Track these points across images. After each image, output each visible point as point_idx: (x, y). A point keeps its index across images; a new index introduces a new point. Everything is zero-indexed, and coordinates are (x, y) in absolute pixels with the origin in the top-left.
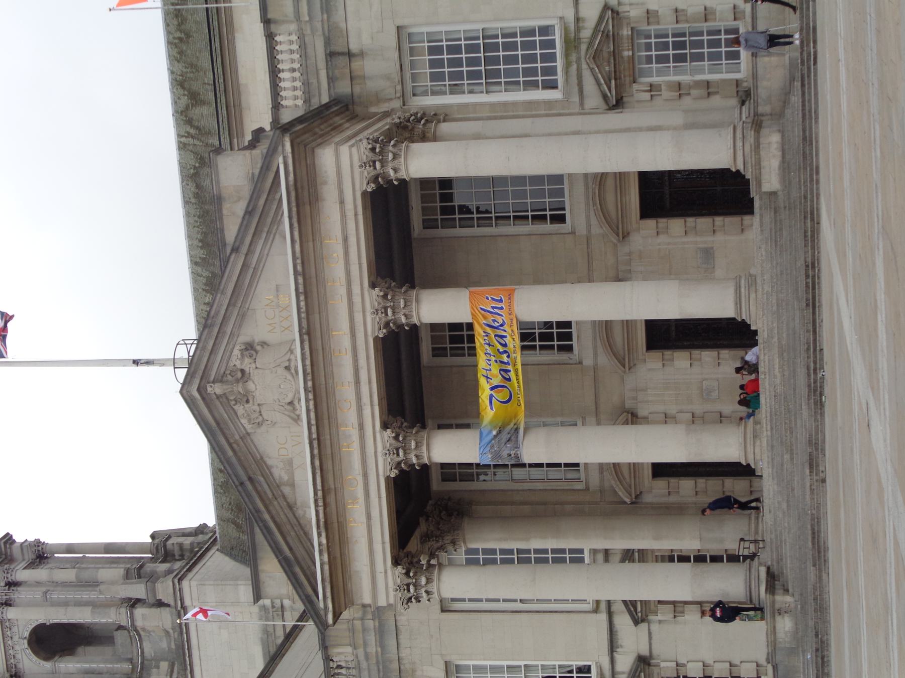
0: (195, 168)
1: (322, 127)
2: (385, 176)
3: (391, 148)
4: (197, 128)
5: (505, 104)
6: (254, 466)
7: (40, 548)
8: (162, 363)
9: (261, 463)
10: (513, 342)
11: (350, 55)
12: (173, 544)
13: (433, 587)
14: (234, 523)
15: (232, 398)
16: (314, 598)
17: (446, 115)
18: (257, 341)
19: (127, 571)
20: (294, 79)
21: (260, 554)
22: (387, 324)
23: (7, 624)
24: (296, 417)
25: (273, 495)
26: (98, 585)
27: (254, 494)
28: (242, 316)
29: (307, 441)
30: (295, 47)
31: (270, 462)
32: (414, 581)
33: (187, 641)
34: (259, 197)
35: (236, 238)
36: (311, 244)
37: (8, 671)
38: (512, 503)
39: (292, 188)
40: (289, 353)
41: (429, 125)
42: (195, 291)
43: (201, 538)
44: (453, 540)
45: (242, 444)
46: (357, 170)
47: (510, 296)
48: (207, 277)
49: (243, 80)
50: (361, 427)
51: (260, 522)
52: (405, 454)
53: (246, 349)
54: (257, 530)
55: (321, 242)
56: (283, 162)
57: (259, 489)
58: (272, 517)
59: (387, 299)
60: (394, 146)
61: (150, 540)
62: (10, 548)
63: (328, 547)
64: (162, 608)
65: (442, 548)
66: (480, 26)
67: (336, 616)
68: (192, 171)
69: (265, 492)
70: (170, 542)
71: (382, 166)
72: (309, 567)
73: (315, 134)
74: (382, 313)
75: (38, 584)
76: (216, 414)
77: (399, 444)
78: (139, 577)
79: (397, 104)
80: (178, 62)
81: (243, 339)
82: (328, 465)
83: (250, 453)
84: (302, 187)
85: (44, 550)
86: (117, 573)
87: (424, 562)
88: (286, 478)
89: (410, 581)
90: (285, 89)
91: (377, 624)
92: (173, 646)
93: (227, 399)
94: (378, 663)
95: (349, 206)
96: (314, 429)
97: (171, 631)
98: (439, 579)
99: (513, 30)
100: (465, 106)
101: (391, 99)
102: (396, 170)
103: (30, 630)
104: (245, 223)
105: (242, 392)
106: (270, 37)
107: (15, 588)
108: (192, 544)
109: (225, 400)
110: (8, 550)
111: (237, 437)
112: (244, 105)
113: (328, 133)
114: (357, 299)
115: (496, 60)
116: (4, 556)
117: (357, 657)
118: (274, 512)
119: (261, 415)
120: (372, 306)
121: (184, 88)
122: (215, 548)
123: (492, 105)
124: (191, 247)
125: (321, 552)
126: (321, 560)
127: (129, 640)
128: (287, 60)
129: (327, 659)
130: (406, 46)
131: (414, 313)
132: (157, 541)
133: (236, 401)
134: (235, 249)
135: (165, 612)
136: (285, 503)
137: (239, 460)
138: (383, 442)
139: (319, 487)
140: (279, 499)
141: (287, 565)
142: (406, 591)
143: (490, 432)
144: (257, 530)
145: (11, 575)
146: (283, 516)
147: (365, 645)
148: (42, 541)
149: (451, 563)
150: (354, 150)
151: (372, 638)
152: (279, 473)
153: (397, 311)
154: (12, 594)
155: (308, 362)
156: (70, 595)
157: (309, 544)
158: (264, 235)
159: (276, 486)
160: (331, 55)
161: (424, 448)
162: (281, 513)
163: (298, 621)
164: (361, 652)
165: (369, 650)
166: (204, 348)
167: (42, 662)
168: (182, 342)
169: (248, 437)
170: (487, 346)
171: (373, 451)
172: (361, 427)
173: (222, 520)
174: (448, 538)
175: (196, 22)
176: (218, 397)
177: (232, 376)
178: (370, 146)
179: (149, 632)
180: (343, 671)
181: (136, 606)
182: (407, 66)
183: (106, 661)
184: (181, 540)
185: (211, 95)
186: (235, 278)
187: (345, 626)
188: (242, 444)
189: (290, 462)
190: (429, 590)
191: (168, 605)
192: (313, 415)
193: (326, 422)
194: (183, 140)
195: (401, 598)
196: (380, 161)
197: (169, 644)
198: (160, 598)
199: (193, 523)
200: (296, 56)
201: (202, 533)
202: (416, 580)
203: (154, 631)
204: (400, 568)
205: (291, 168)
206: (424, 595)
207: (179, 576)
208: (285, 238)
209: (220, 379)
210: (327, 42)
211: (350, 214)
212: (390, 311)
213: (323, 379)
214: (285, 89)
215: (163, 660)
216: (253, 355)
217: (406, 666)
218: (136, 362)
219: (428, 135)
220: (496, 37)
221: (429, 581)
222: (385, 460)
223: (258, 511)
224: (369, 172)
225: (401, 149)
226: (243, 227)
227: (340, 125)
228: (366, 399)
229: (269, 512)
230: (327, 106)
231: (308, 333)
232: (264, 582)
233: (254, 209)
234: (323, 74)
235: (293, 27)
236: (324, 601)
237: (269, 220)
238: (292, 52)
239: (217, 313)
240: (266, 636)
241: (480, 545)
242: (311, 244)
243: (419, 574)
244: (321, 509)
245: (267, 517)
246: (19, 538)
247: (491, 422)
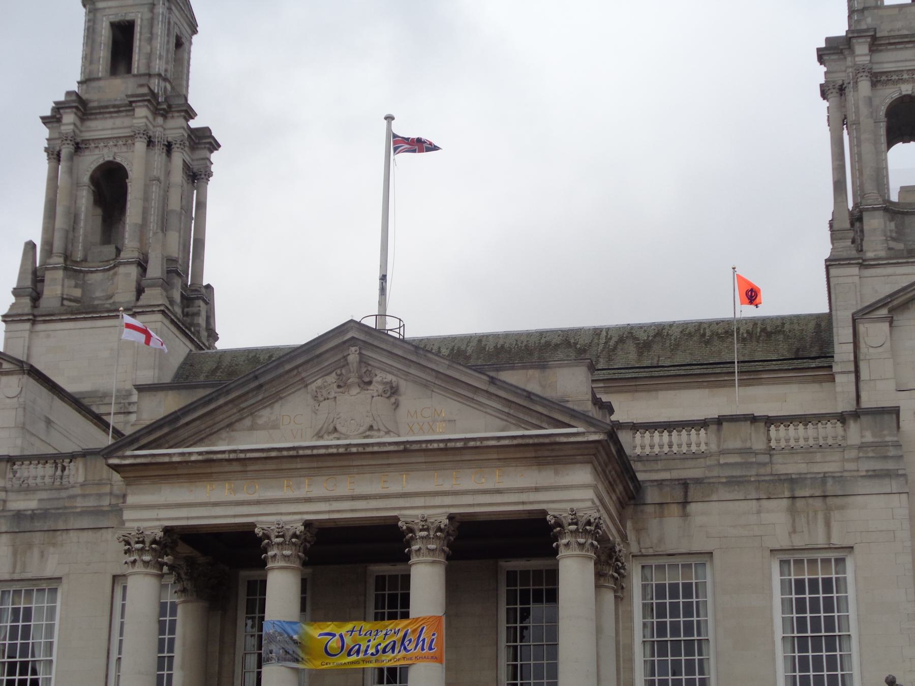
0: (576, 344)
1: (613, 473)
2: (561, 534)
3: (590, 541)
4: (615, 348)
5: (631, 660)
6: (274, 390)
7: (203, 176)
8: (382, 303)
9: (277, 397)
10: (388, 661)
11: (685, 503)
12: (200, 307)
13: (138, 568)
14: (217, 368)
15: (344, 371)
16: (136, 446)
17: (622, 599)
18: (400, 398)
19: (174, 260)
20: (661, 446)
21: (184, 393)
22: (411, 530)
23: (130, 142)
24: (320, 435)
25: (244, 409)
26: (162, 230)
27: (246, 389)
28: (425, 385)
29: (296, 444)
30: (694, 448)
31: (277, 406)
32: (147, 548)
33: (100, 317)
34: (544, 406)
35: (504, 382)
36: (495, 456)
37: (83, 140)
38: (221, 653)
39: (552, 439)
40: (386, 430)
41: (612, 580)
42: (453, 339)
43: (204, 334)
44: (187, 590)
45: (298, 379)
46: (568, 506)
47: (435, 659)
48: (465, 351)
49: (663, 395)
50: (308, 500)
51: (216, 394)
52: (278, 544)
53: (392, 388)
54: (208, 391)
55: (497, 467)
56: (578, 432)
57: (250, 395)
58: (220, 407)
59: (436, 532)
60: (592, 544)
61: (205, 284)
62: (205, 148)
63: (187, 462)
64: (135, 293)
65: (179, 579)
66: (711, 637)
67: (116, 468)
68: (572, 341)
69: (246, 401)
70: (201, 303)
71: (571, 532)
72: (167, 442)
73: (606, 466)
74: (423, 526)
75: (168, 173)
76: (327, 355)
77: (288, 538)
78: (169, 272)
79: (634, 549)
80: (681, 332)
81: (403, 385)
82: (271, 466)
83: (287, 387)
84: (553, 450)
85: (201, 180)
86: (174, 250)
87: (166, 559)
88: (260, 422)
89: (147, 544)
90: (652, 437)
91: (106, 509)
92: (96, 302)
93: (343, 366)
94: (65, 508)
95: (533, 497)
96: (308, 452)
97: (111, 301)
98: (147, 574)
99: (706, 671)
100: (631, 619)
101: (639, 543)
102: (567, 545)
103: (122, 163)
104: (519, 391)
105: (349, 381)
106: (704, 424)
107: (165, 151)
108: (198, 325)
109: (342, 364)
110: (203, 146)
111: (304, 375)
112: (637, 395)
113: (607, 477)
114: (438, 501)
115: (676, 652)
116: (197, 141)
117: (73, 487)
118: (226, 409)
119: (325, 399)
120: (430, 516)
121: (655, 336)
122: (193, 348)
123: (630, 647)
124: (496, 336)
125: (183, 454)
126: (174, 454)
127: (106, 259)
128: (681, 440)
129: (72, 457)
130: (692, 560)
131: (421, 559)
132: (204, 291)
133: (340, 375)
134: (493, 381)
135: (131, 296)
136: (234, 420)
137: (281, 376)
138: (291, 522)
139: (249, 455)
140: (238, 414)
141: (172, 419)
142: (137, 539)
143: (296, 633)
144: (208, 391)
145: (178, 148)
146: (221, 417)
147: (84, 496)
148: (211, 179)
149: (163, 587)
150: (589, 504)
151: (91, 503)
152: (265, 415)
153: (425, 541)
154: (159, 148)
155: (376, 449)
156: (155, 203)
157: (191, 443)
158: (506, 410)
159: (252, 411)
160: (685, 484)
161: (283, 564)
162: (224, 416)
163: (114, 428)
164: (77, 491)
165: (79, 499)
166: (394, 345)
167: (88, 174)
168: (402, 325)
169: (303, 385)
170: (384, 632)
171: (283, 511)
172: (308, 500)
173: (221, 356)
174: (189, 585)
175: (720, 352)
176: (345, 357)
177: (365, 373)
178: (592, 520)
179: (112, 279)
180: (59, 472)
181: (139, 268)
182: (672, 560)
183: (85, 236)
184: (203, 314)
185: (646, 363)
186: (464, 379)
187: (105, 475)
188: (298, 379)
189: (275, 427)
190: (137, 564)
191: (138, 299)
192: (322, 451)
193: (315, 465)
194: (604, 333)
195: (130, 534)
196: (577, 529)
197: (99, 298)
198: (146, 292)
199: (220, 327)
200: (684, 449)
201: (209, 336)
202: (148, 551)
203: (113, 284)
204: (161, 534)
205: (572, 439)
206: (132, 559)
207: (167, 312)
208: (502, 430)
209: (362, 360)
210: (698, 481)
211: (524, 497)
212: (424, 533)
213: (359, 463)
214: (652, 437)
215: (83, 292)
216: (385, 394)
217: (60, 537)
218: (383, 278)
219: (602, 579)
220: (700, 654)
221: (146, 564)
222: (272, 523)
223: (228, 392)
224: (566, 518)
225: (588, 551)
226: (513, 389)
227: (614, 491)
228: (336, 506)
229: (226, 404)
230: (634, 478)
231: (405, 450)
232: (155, 396)
233: (532, 401)
234: (666, 475)
235: (714, 447)
236: (133, 455)
237: (521, 416)
238: (689, 445)
239: (429, 360)
240: (100, 395)
241: (179, 618)
242: (495, 456)
243: (154, 554)
244: (226, 456)
245: (221, 401)
246: (215, 157)
247: (306, 634)
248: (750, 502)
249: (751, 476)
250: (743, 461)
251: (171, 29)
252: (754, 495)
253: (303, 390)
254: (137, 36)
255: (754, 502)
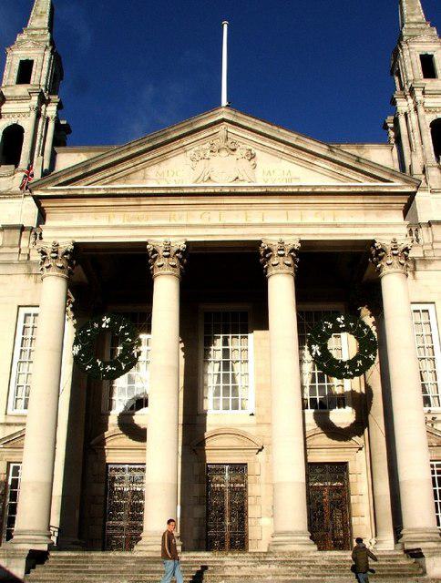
13: (54, 272)
16: (56, 183)
31: (163, 164)
98: (58, 276)
253: (182, 155)
254: (34, 66)
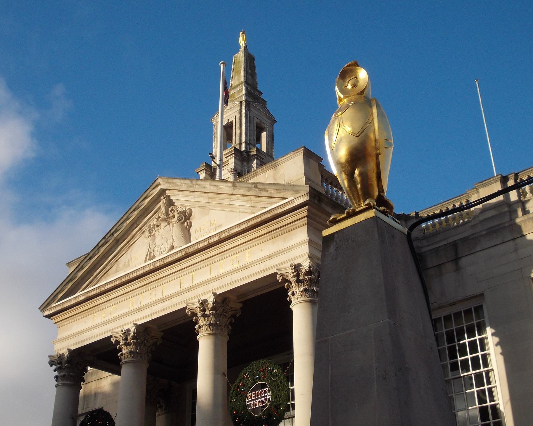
11: (456, 259)
152: (123, 259)
160: (455, 245)
202: (64, 368)
248: (508, 244)
249: (505, 223)
250: (498, 213)
251: (252, 119)
252: (510, 237)
255: (511, 243)
